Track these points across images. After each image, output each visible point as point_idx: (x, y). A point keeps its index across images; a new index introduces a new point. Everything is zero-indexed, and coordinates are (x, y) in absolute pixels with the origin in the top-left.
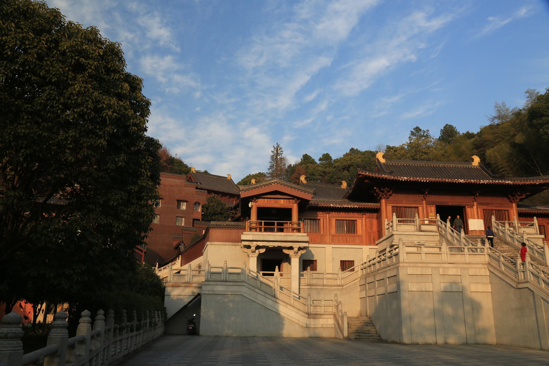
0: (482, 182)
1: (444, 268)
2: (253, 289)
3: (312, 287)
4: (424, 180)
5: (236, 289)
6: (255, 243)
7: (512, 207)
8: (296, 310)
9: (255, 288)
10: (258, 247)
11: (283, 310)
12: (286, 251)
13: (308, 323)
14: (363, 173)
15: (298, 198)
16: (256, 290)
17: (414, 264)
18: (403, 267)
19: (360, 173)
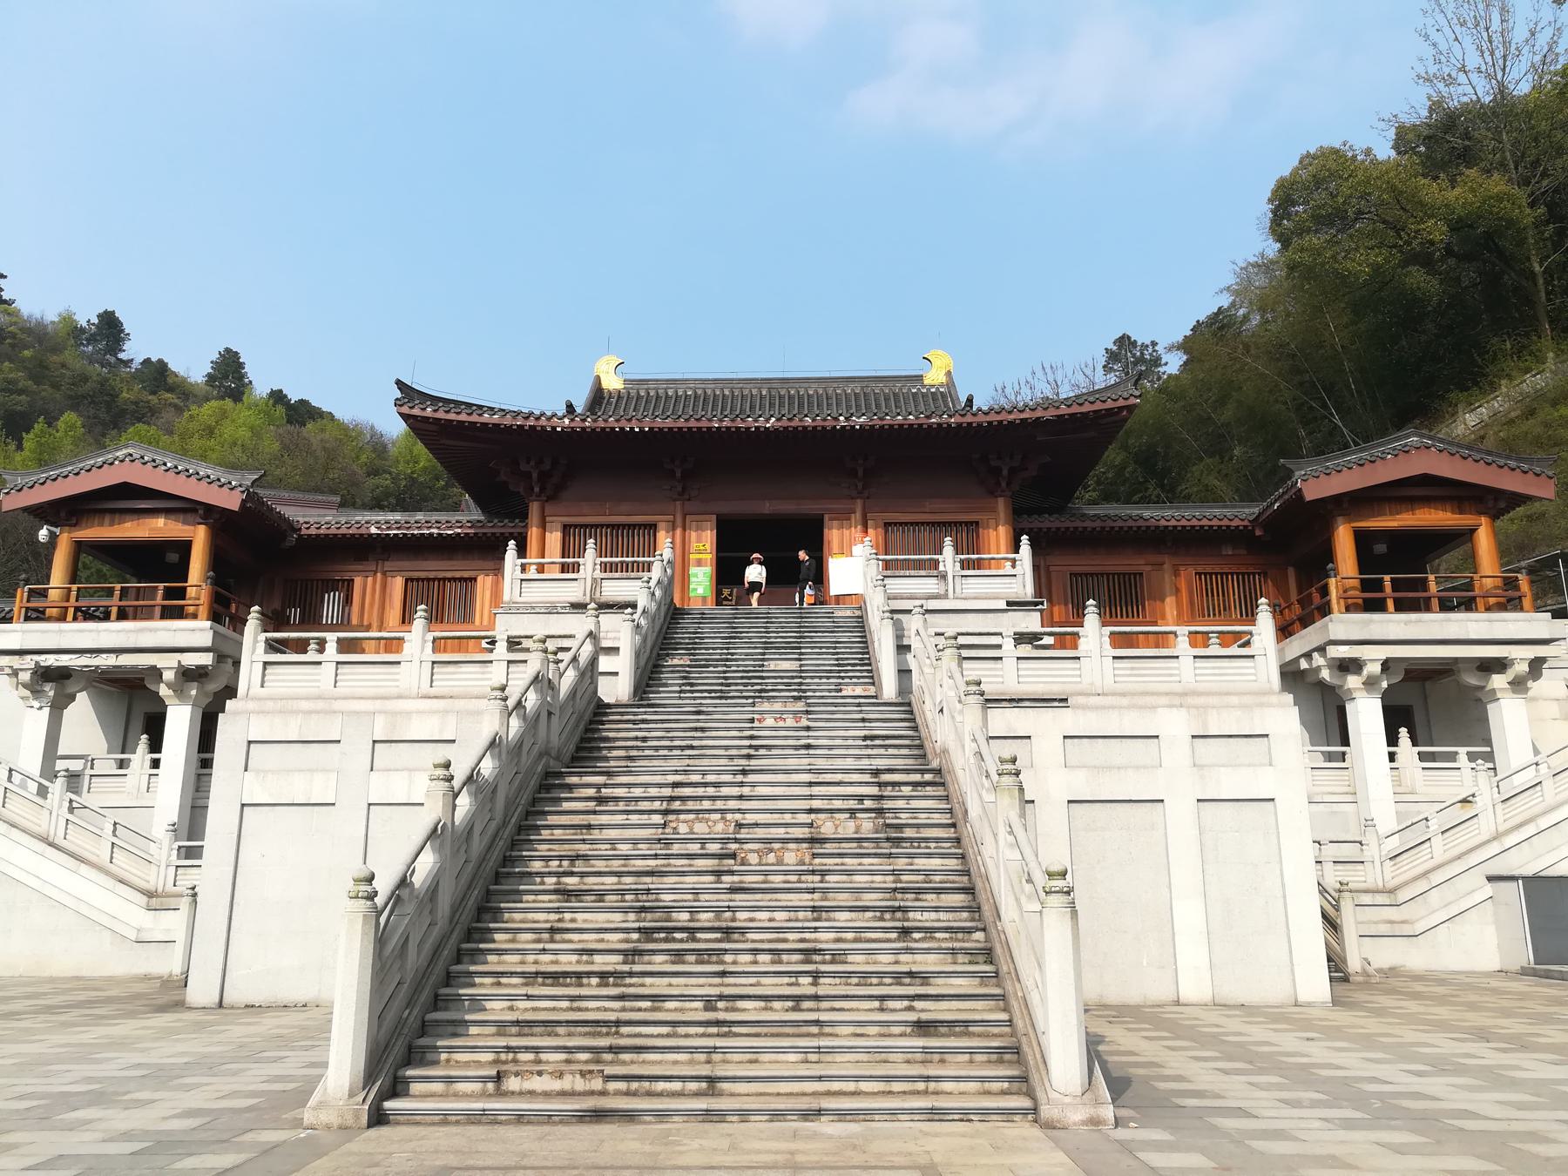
1: (394, 713)
6: (29, 662)
10: (46, 675)
18: (236, 713)
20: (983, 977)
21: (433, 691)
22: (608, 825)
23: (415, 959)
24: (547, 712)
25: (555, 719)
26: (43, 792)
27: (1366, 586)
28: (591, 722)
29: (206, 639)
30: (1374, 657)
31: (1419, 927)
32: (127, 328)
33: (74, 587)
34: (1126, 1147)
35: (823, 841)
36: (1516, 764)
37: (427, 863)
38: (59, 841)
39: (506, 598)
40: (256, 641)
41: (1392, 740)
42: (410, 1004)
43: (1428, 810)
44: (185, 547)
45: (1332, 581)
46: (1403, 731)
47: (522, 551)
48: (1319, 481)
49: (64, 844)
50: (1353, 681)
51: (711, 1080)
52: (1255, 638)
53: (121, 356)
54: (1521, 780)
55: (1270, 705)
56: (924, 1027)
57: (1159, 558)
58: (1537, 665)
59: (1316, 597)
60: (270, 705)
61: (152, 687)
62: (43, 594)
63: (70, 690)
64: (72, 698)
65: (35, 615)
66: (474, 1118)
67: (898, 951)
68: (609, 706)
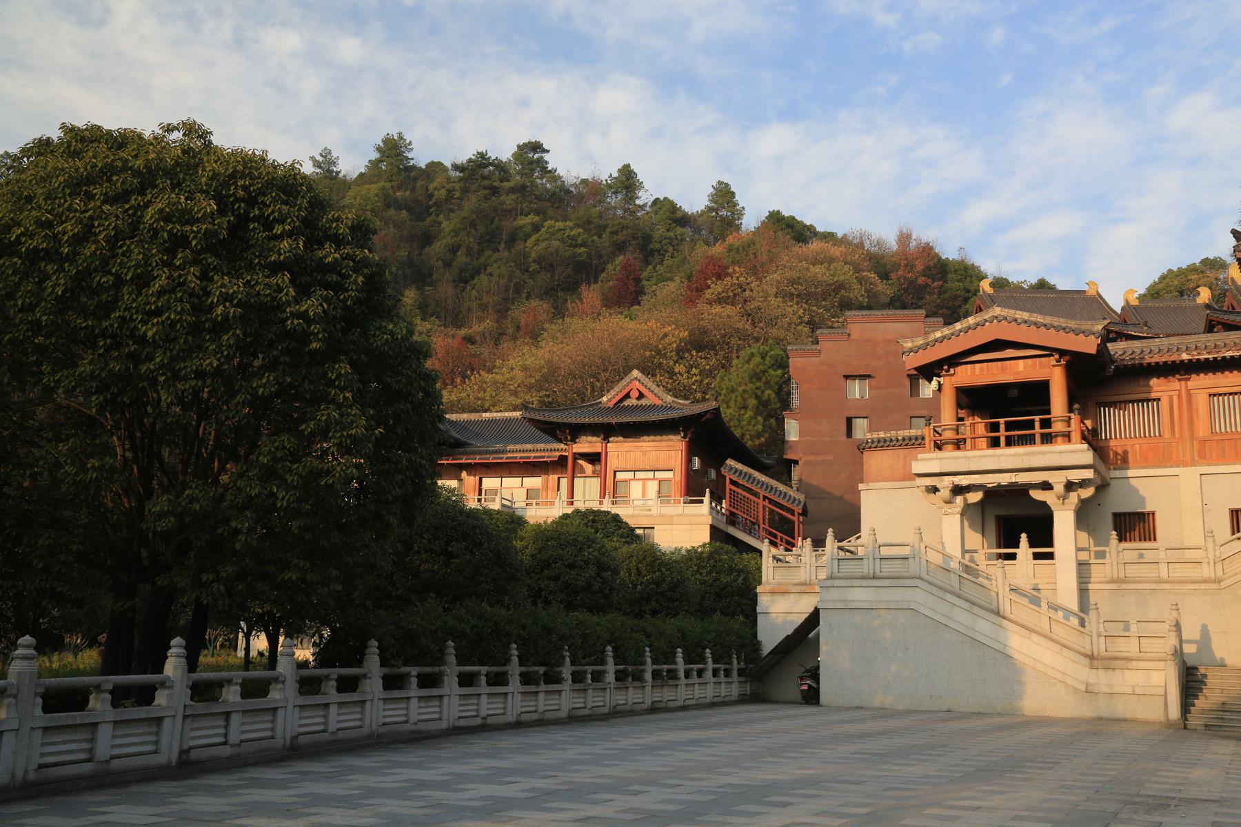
2: (940, 593)
3: (1124, 586)
5: (898, 595)
6: (947, 482)
8: (1058, 647)
9: (947, 591)
10: (958, 490)
11: (1019, 644)
12: (1036, 495)
13: (1093, 681)
15: (1062, 353)
16: (949, 597)
32: (640, 177)
38: (1007, 614)
49: (1012, 617)
53: (638, 202)
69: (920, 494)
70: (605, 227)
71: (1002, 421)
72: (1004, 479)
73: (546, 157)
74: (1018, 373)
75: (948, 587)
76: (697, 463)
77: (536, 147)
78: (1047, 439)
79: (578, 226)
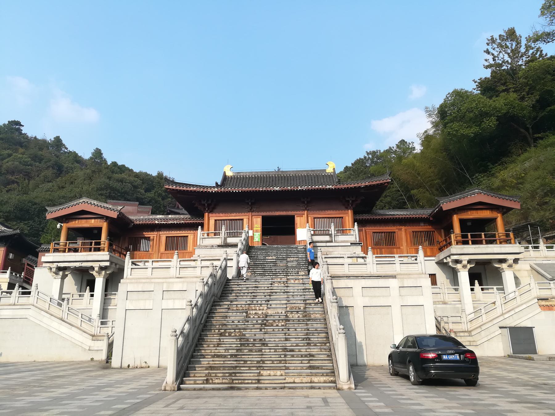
0: (299, 188)
1: (169, 283)
4: (236, 190)
6: (55, 265)
7: (348, 213)
10: (59, 269)
14: (170, 187)
17: (136, 280)
18: (124, 283)
19: (167, 187)
20: (328, 356)
21: (180, 276)
22: (230, 314)
23: (185, 351)
24: (214, 283)
25: (216, 286)
26: (60, 305)
27: (463, 236)
28: (225, 285)
29: (107, 258)
30: (465, 259)
31: (478, 343)
33: (68, 242)
34: (355, 393)
35: (289, 321)
36: (510, 291)
37: (187, 327)
38: (65, 320)
39: (198, 244)
40: (129, 262)
41: (472, 284)
42: (184, 362)
43: (482, 307)
44: (100, 229)
45: (452, 235)
46: (476, 281)
47: (202, 229)
48: (447, 205)
50: (459, 266)
51: (259, 380)
52: (418, 258)
54: (512, 296)
55: (422, 278)
56: (311, 368)
57: (401, 227)
58: (516, 261)
59: (448, 239)
60: (133, 281)
61: (91, 272)
62: (58, 244)
63: (67, 273)
64: (67, 275)
65: (56, 250)
66: (200, 389)
67: (306, 349)
68: (230, 280)
69: (47, 271)
70: (43, 159)
71: (94, 241)
72: (77, 265)
73: (22, 128)
74: (91, 224)
75: (44, 309)
76: (11, 256)
77: (18, 123)
78: (99, 250)
79: (30, 157)
